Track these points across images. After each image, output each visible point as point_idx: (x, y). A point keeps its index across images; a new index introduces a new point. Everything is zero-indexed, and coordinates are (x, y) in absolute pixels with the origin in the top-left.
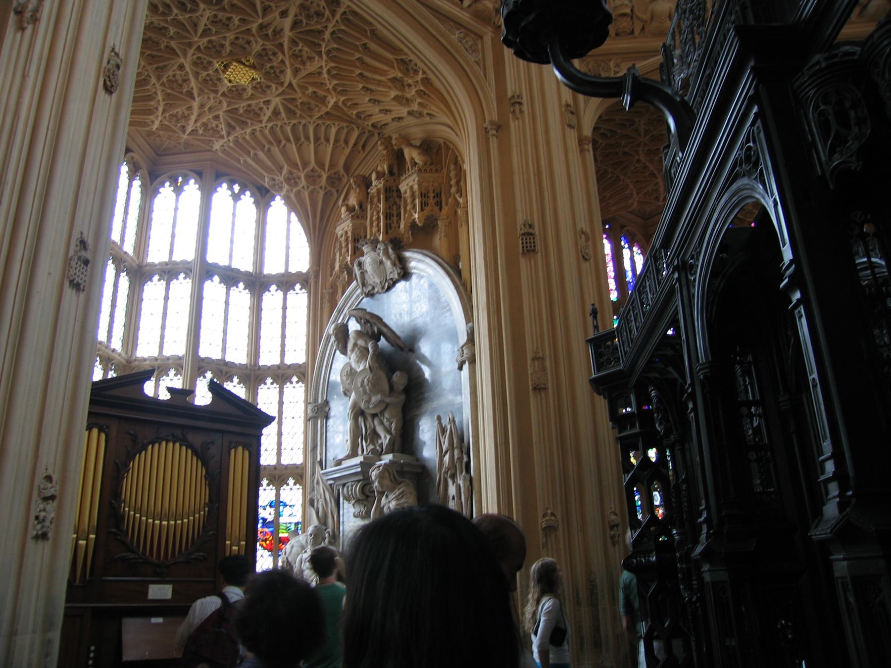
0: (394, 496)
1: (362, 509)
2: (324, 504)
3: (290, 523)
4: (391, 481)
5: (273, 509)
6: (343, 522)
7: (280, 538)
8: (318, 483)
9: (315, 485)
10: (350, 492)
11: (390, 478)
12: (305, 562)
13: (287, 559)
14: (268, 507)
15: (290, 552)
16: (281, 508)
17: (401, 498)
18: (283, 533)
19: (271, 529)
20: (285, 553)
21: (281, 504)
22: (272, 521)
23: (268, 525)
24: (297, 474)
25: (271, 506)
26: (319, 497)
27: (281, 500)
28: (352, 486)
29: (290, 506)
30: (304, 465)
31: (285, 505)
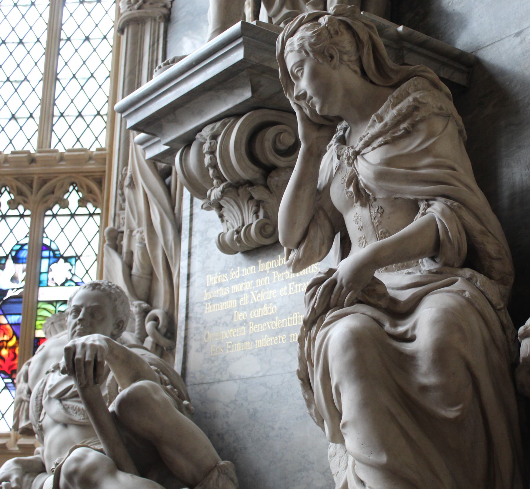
0: (378, 126)
1: (250, 219)
2: (146, 242)
4: (364, 74)
5: (21, 267)
6: (189, 276)
8: (132, 185)
9: (127, 191)
10: (207, 159)
11: (360, 60)
14: (10, 262)
16: (45, 263)
17: (408, 133)
19: (14, 319)
21: (46, 253)
22: (19, 297)
23: (6, 307)
24: (88, 175)
25: (16, 260)
26: (134, 224)
27: (46, 242)
28: (214, 137)
29: (66, 259)
30: (107, 152)
31: (56, 257)
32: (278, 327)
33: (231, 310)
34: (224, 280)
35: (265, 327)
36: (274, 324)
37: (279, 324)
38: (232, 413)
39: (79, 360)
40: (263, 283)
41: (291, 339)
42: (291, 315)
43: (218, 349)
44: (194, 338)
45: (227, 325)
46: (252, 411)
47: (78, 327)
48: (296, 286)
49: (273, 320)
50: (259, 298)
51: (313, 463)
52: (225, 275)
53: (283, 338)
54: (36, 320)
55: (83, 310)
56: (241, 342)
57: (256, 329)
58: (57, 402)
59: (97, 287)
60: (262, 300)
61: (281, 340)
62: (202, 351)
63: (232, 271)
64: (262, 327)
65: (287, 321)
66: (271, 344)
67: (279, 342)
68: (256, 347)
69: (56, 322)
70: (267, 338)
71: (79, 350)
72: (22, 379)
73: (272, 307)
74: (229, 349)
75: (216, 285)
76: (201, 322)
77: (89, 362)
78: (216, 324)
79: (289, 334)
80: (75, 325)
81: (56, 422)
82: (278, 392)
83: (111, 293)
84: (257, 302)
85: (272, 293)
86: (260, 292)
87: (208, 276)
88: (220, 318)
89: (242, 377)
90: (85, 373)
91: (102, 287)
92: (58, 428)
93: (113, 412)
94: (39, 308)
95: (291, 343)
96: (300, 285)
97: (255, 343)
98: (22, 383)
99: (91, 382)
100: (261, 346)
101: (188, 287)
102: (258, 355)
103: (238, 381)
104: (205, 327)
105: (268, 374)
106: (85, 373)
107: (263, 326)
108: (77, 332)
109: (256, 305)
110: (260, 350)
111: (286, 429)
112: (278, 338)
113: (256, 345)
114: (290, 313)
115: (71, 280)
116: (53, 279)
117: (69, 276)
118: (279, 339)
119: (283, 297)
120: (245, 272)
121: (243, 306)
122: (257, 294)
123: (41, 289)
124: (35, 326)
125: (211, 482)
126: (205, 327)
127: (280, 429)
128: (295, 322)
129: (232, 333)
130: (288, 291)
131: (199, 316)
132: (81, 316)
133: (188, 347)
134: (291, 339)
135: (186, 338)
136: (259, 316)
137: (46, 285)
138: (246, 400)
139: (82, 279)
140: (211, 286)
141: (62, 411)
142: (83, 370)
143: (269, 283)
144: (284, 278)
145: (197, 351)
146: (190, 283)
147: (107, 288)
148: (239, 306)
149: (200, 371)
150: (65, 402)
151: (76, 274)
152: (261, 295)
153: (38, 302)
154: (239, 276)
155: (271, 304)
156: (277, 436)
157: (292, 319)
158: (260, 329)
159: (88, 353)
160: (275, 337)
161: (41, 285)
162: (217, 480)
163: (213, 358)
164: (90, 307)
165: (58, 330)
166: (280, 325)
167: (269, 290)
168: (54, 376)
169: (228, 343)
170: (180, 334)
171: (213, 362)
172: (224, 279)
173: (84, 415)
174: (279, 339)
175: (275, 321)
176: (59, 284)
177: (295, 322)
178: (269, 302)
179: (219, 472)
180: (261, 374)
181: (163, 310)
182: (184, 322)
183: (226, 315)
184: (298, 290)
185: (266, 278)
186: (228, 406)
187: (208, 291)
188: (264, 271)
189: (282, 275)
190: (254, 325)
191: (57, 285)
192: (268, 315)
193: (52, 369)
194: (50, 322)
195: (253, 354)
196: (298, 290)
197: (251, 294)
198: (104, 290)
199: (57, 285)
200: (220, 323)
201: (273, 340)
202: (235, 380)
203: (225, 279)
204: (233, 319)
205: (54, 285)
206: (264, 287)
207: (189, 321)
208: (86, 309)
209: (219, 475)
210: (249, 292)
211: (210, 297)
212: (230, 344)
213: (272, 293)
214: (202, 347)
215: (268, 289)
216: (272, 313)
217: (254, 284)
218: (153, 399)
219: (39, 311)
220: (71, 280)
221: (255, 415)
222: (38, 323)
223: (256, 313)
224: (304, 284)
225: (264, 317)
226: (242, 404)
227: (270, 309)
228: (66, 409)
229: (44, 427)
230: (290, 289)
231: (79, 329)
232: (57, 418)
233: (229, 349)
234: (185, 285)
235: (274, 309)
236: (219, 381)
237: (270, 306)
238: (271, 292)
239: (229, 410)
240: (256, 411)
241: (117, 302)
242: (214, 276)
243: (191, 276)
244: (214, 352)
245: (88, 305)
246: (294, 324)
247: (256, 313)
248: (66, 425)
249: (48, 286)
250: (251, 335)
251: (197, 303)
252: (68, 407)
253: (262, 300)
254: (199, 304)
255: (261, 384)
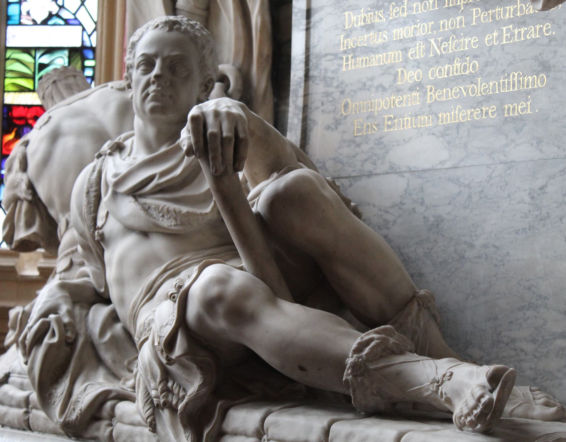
3: (50, 50)
6: (309, 13)
7: (10, 107)
12: (115, 194)
13: (31, 186)
15: (46, 160)
18: (23, 89)
20: (24, 167)
32: (481, 93)
33: (392, 66)
34: (377, 20)
35: (456, 94)
36: (473, 91)
37: (482, 89)
38: (394, 222)
39: (212, 134)
40: (452, 26)
41: (506, 112)
42: (506, 75)
43: (368, 126)
44: (322, 108)
45: (384, 89)
46: (432, 219)
47: (152, 88)
48: (516, 32)
49: (472, 83)
50: (444, 49)
51: (546, 298)
52: (380, 13)
53: (490, 111)
54: (5, 78)
55: (158, 63)
56: (411, 116)
57: (439, 97)
58: (131, 199)
59: (176, 27)
60: (450, 51)
61: (487, 113)
62: (337, 128)
63: (394, 7)
64: (451, 93)
65: (499, 85)
66: (469, 119)
67: (484, 117)
68: (440, 124)
69: (60, 80)
70: (460, 110)
71: (210, 120)
72: (16, 165)
73: (470, 63)
74: (389, 127)
75: (362, 27)
76: (335, 84)
77: (228, 139)
78: (364, 87)
79: (502, 103)
80: (148, 85)
81: (129, 229)
82: (481, 192)
83: (196, 36)
84: (442, 56)
85: (470, 41)
86: (447, 40)
87: (346, 13)
88: (372, 79)
89: (412, 169)
90: (223, 155)
91: (183, 28)
92: (131, 239)
93: (258, 214)
94: (8, 59)
95: (506, 118)
96: (523, 30)
97: (438, 117)
98: (17, 172)
99: (230, 169)
100: (449, 122)
101: (308, 29)
102: (443, 136)
103: (407, 175)
104: (342, 93)
105: (462, 164)
106: (223, 155)
107: (453, 91)
108: (152, 95)
109: (438, 60)
110: (447, 128)
111: (496, 247)
112: (482, 110)
113: (440, 120)
114: (503, 72)
115: (58, 15)
116: (28, 13)
117: (55, 10)
118: (484, 112)
119: (491, 47)
120: (417, 7)
121: (415, 60)
122: (442, 42)
123: (10, 29)
124: (4, 87)
125: (410, 319)
126: (342, 93)
127: (485, 246)
128: (514, 86)
129: (394, 101)
130: (500, 38)
131: (329, 74)
132: (156, 71)
133: (309, 122)
134: (506, 112)
135: (305, 108)
136: (446, 76)
137: (17, 22)
138: (422, 204)
139: (74, 14)
140: (351, 30)
141: (142, 213)
142: (220, 150)
143: (463, 26)
144: (493, 17)
145: (328, 128)
146: (312, 24)
147: (189, 28)
148: (406, 60)
149: (334, 159)
150: (143, 200)
151: (65, 6)
152: (449, 44)
153: (7, 48)
154: (405, 14)
155: (468, 58)
156: (480, 257)
157: (509, 83)
158: (447, 96)
159: (225, 126)
160: (475, 108)
161: (9, 22)
162: (417, 316)
163: (358, 140)
164: (168, 57)
165: (64, 93)
166: (485, 91)
167: (465, 36)
168: (114, 161)
169: (386, 117)
170: (294, 102)
171: (358, 146)
172: (379, 18)
173: (176, 219)
174: (484, 112)
175: (476, 84)
176: (39, 22)
177: (514, 86)
178: (463, 55)
179: (419, 305)
180: (448, 165)
181: (233, 65)
182: (303, 85)
183: (383, 74)
184: (519, 37)
185: (458, 18)
186: (387, 212)
187: (347, 37)
188: (453, 6)
189: (489, 14)
190: (436, 90)
191: (35, 23)
192: (463, 75)
193: (109, 151)
194: (52, 81)
195: (433, 134)
196: (519, 37)
197: (430, 42)
198: (186, 32)
199: (35, 23)
200: (370, 86)
201: (472, 113)
202: (400, 173)
203: (381, 19)
204: (395, 80)
205: (31, 23)
206: (454, 32)
207: (311, 83)
208: (164, 60)
209: (420, 310)
210: (426, 40)
211: (351, 45)
212: (390, 119)
213: (470, 41)
214: (338, 123)
215: (462, 34)
216: (470, 72)
217: (436, 28)
218: (323, 197)
219: (8, 62)
220: (58, 15)
221: (438, 225)
222: (7, 81)
223: (440, 71)
224: (531, 28)
225: (455, 79)
226: (414, 210)
227: (465, 66)
228: (146, 209)
229: (106, 235)
230: (505, 35)
231: (154, 91)
232: (132, 222)
233: (389, 127)
234: (303, 27)
235: (474, 66)
236: (370, 175)
237: (465, 61)
238: (467, 40)
239: (390, 218)
240: (439, 220)
241: (205, 51)
242: (360, 13)
243: (312, 12)
244: (359, 131)
245: (166, 54)
246: (511, 90)
247: (440, 71)
248: (145, 234)
249: (20, 24)
250: (430, 106)
251: (326, 55)
252: (149, 208)
253: (450, 51)
254: (329, 57)
255: (449, 180)
